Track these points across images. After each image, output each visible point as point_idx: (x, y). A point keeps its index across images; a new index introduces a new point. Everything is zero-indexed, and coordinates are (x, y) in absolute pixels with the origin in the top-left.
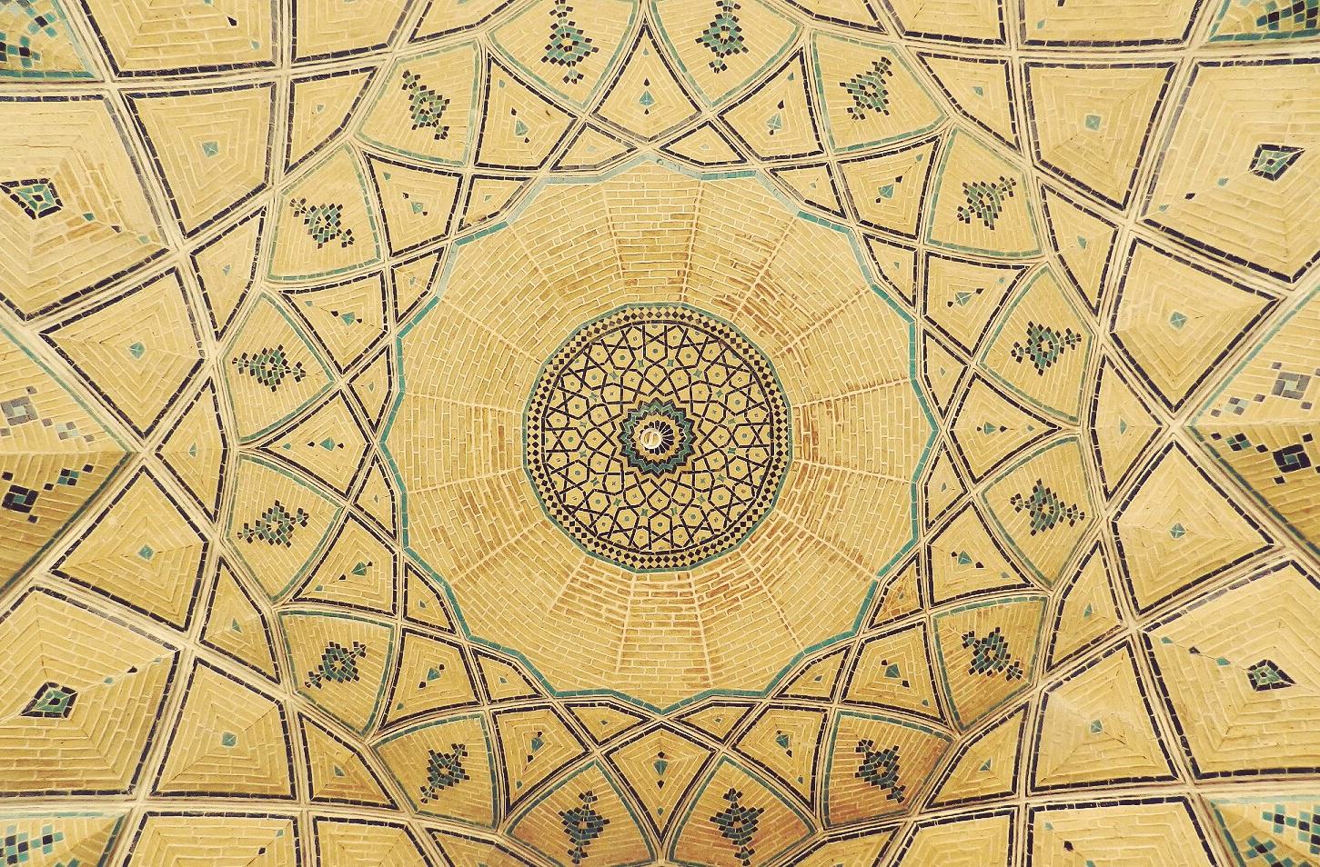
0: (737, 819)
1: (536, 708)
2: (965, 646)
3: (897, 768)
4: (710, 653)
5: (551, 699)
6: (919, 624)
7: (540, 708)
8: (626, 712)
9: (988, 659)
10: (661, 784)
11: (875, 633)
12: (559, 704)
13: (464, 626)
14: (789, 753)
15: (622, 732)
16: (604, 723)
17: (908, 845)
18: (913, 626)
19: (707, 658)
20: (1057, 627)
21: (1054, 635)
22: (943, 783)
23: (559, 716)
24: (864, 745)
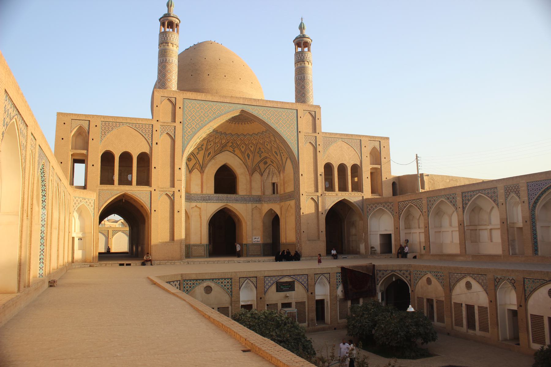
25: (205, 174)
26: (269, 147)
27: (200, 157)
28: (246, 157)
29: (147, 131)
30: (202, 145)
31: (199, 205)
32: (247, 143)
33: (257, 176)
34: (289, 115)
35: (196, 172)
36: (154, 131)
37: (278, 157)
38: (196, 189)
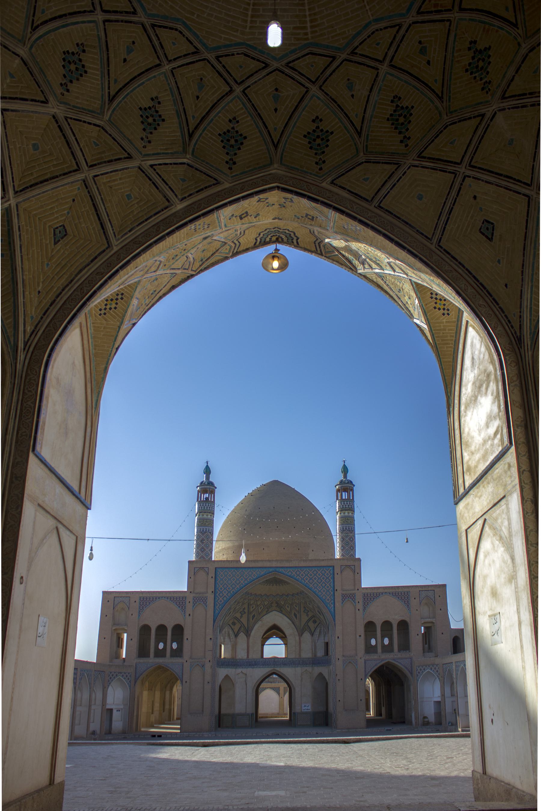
0: (318, 137)
1: (197, 61)
2: (469, 49)
3: (410, 122)
4: (310, 15)
5: (206, 54)
6: (448, 20)
7: (200, 60)
8: (254, 59)
9: (477, 67)
10: (276, 110)
11: (420, 18)
12: (211, 57)
13: (142, 6)
14: (353, 96)
15: (252, 75)
16: (241, 67)
17: (403, 175)
18: (443, 21)
19: (308, 19)
20: (517, 72)
21: (514, 76)
22: (429, 144)
23: (212, 66)
24: (397, 98)
25: (251, 637)
26: (311, 606)
27: (244, 620)
28: (294, 617)
29: (181, 603)
30: (244, 609)
31: (244, 670)
32: (291, 603)
33: (307, 636)
34: (325, 572)
35: (242, 635)
36: (187, 602)
37: (322, 617)
38: (241, 654)
